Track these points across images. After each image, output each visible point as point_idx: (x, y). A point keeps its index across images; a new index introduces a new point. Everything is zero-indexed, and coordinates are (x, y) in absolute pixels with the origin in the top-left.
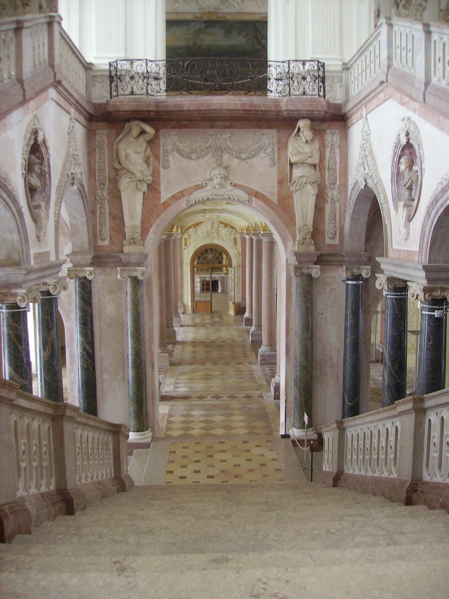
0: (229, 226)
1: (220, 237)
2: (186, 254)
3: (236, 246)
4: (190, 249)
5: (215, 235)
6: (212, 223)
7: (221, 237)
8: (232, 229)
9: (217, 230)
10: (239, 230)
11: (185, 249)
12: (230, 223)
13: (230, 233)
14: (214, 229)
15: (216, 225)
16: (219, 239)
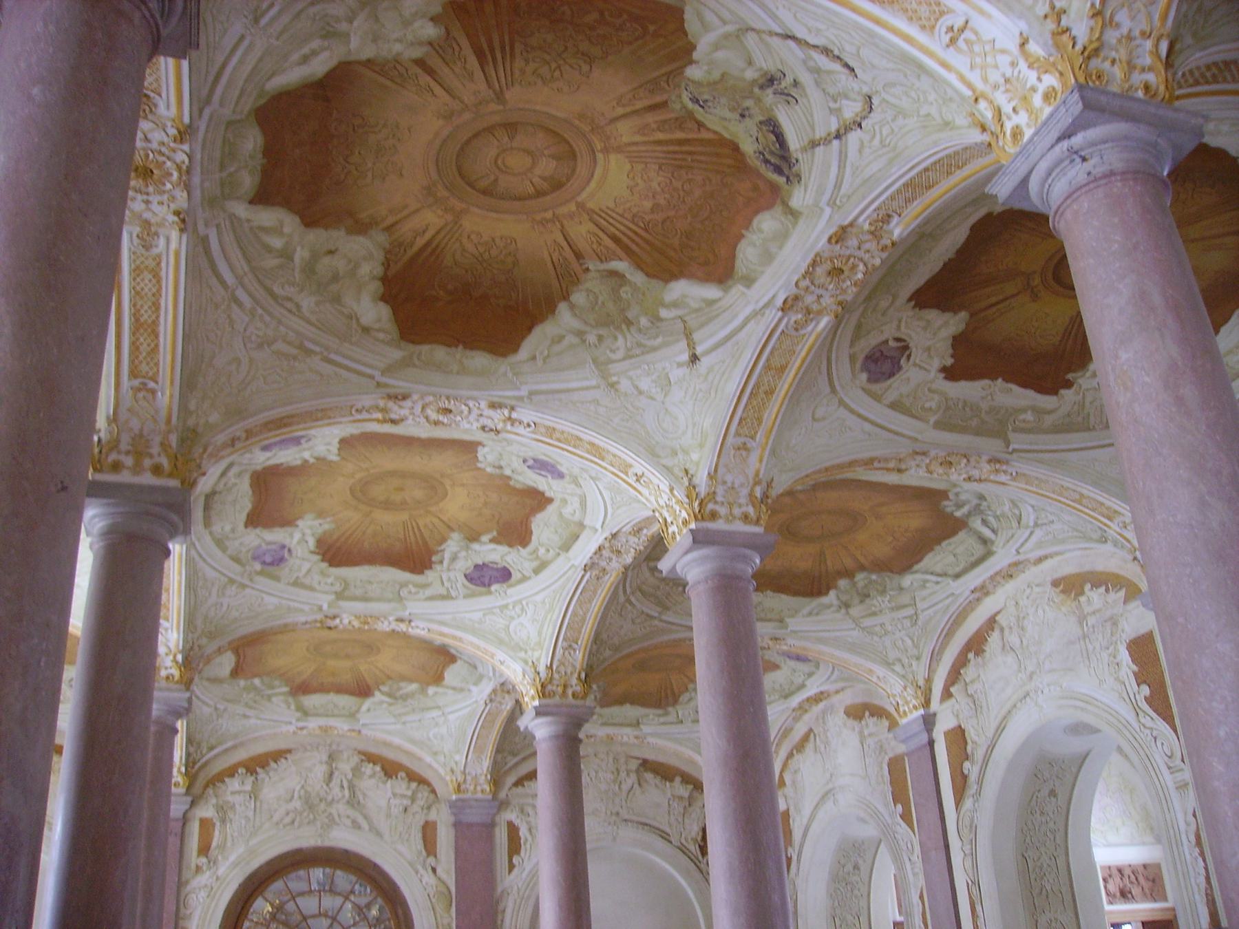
0: (402, 774)
1: (360, 820)
2: (203, 894)
3: (431, 860)
4: (222, 870)
5: (341, 808)
6: (332, 757)
7: (366, 817)
8: (414, 785)
9: (352, 787)
10: (446, 790)
11: (198, 869)
12: (405, 761)
13: (406, 802)
14: (335, 782)
15: (345, 766)
16: (356, 825)
